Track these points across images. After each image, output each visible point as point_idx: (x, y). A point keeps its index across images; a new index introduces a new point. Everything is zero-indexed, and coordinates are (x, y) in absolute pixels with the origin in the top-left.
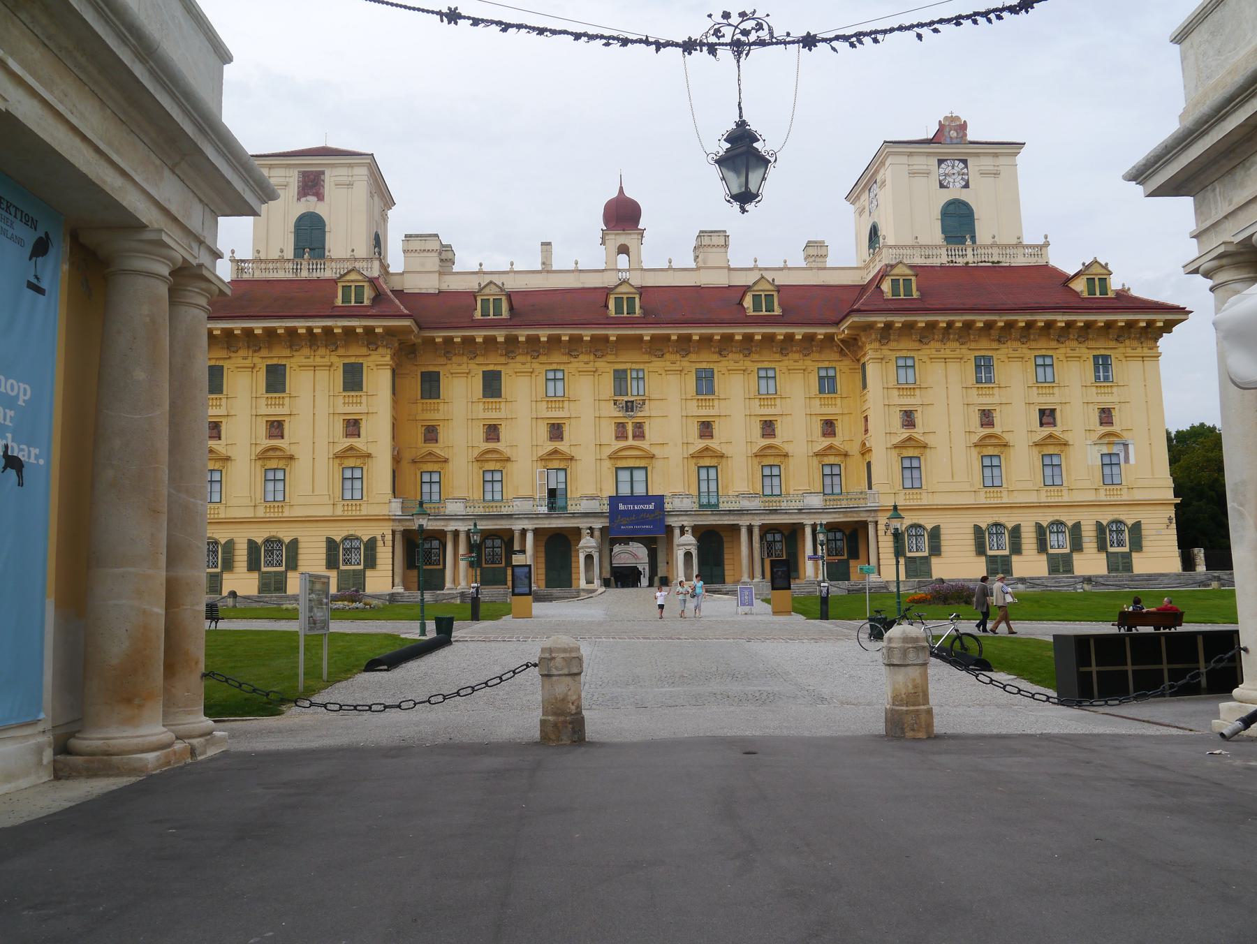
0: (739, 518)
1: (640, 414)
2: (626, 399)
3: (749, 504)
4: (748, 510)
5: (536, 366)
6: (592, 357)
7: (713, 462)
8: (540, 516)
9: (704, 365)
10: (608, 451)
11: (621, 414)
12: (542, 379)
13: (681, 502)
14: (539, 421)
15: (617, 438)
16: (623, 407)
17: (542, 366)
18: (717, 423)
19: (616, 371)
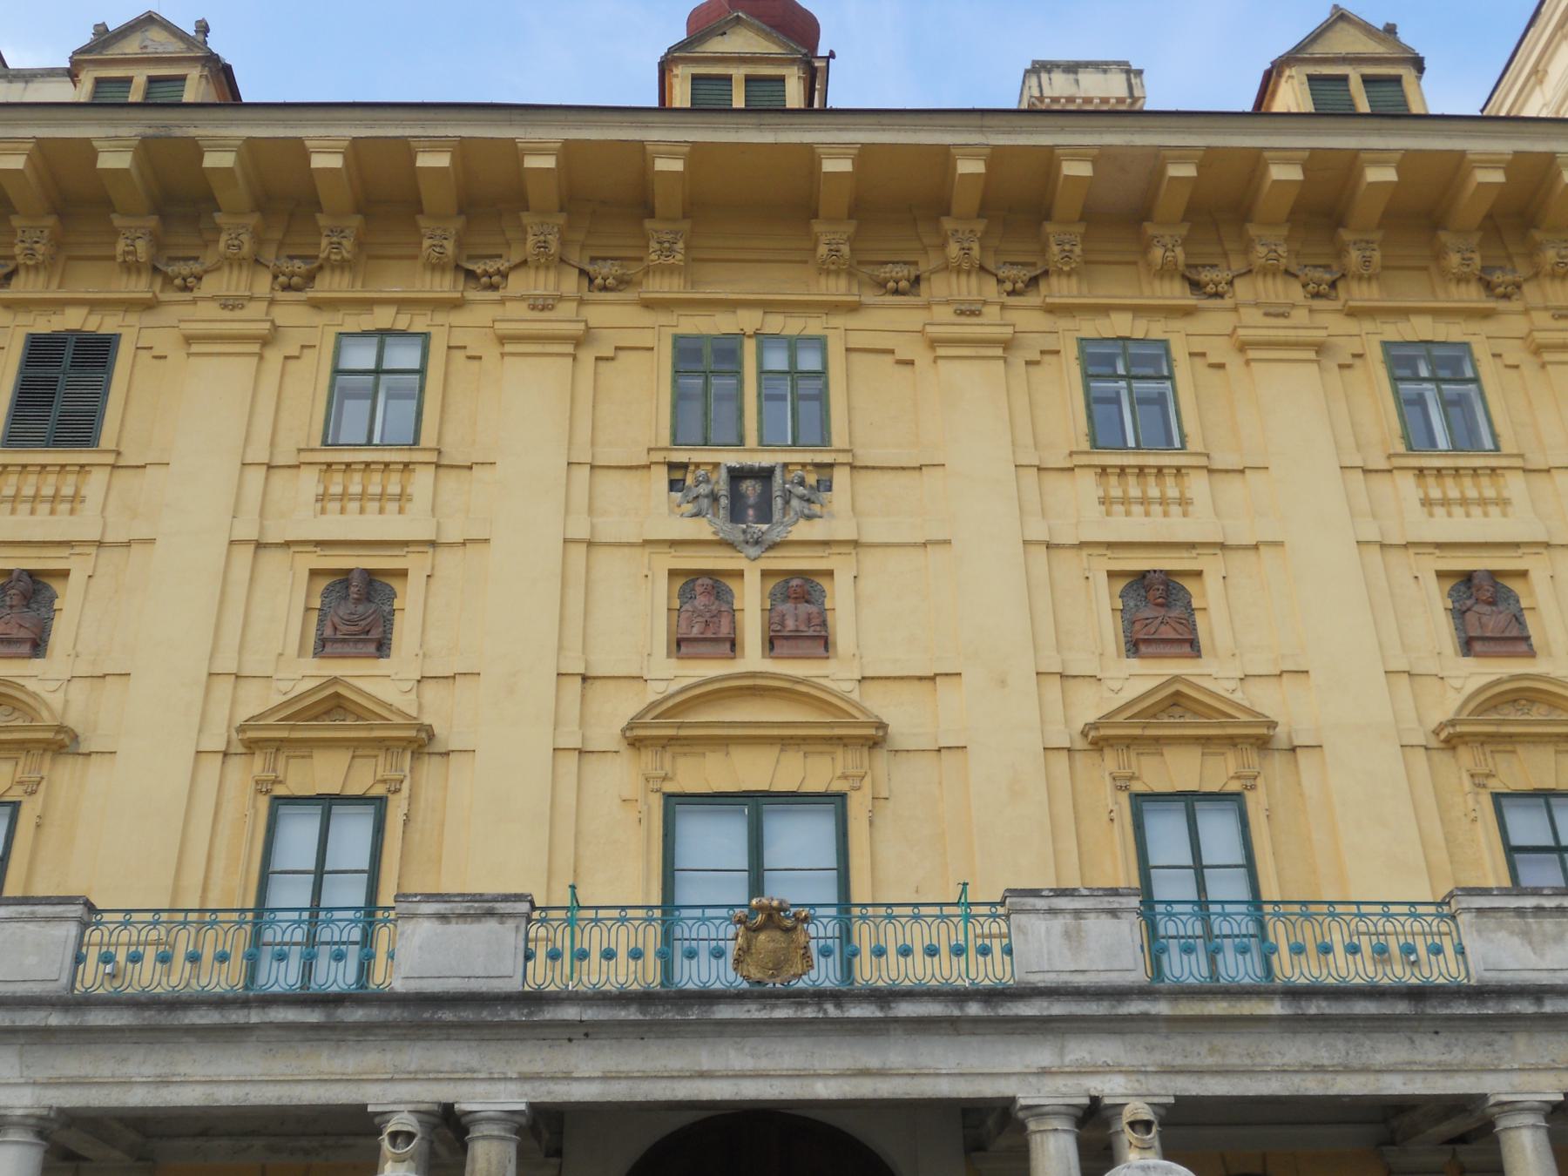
0: (1479, 1057)
1: (802, 531)
2: (732, 459)
3: (1533, 960)
4: (1538, 993)
5: (291, 314)
6: (570, 283)
7: (1217, 773)
8: (97, 1018)
9: (1121, 325)
10: (619, 707)
11: (702, 529)
12: (311, 377)
13: (1073, 938)
14: (272, 559)
15: (680, 645)
16: (714, 497)
17: (321, 319)
18: (1212, 582)
19: (688, 354)
